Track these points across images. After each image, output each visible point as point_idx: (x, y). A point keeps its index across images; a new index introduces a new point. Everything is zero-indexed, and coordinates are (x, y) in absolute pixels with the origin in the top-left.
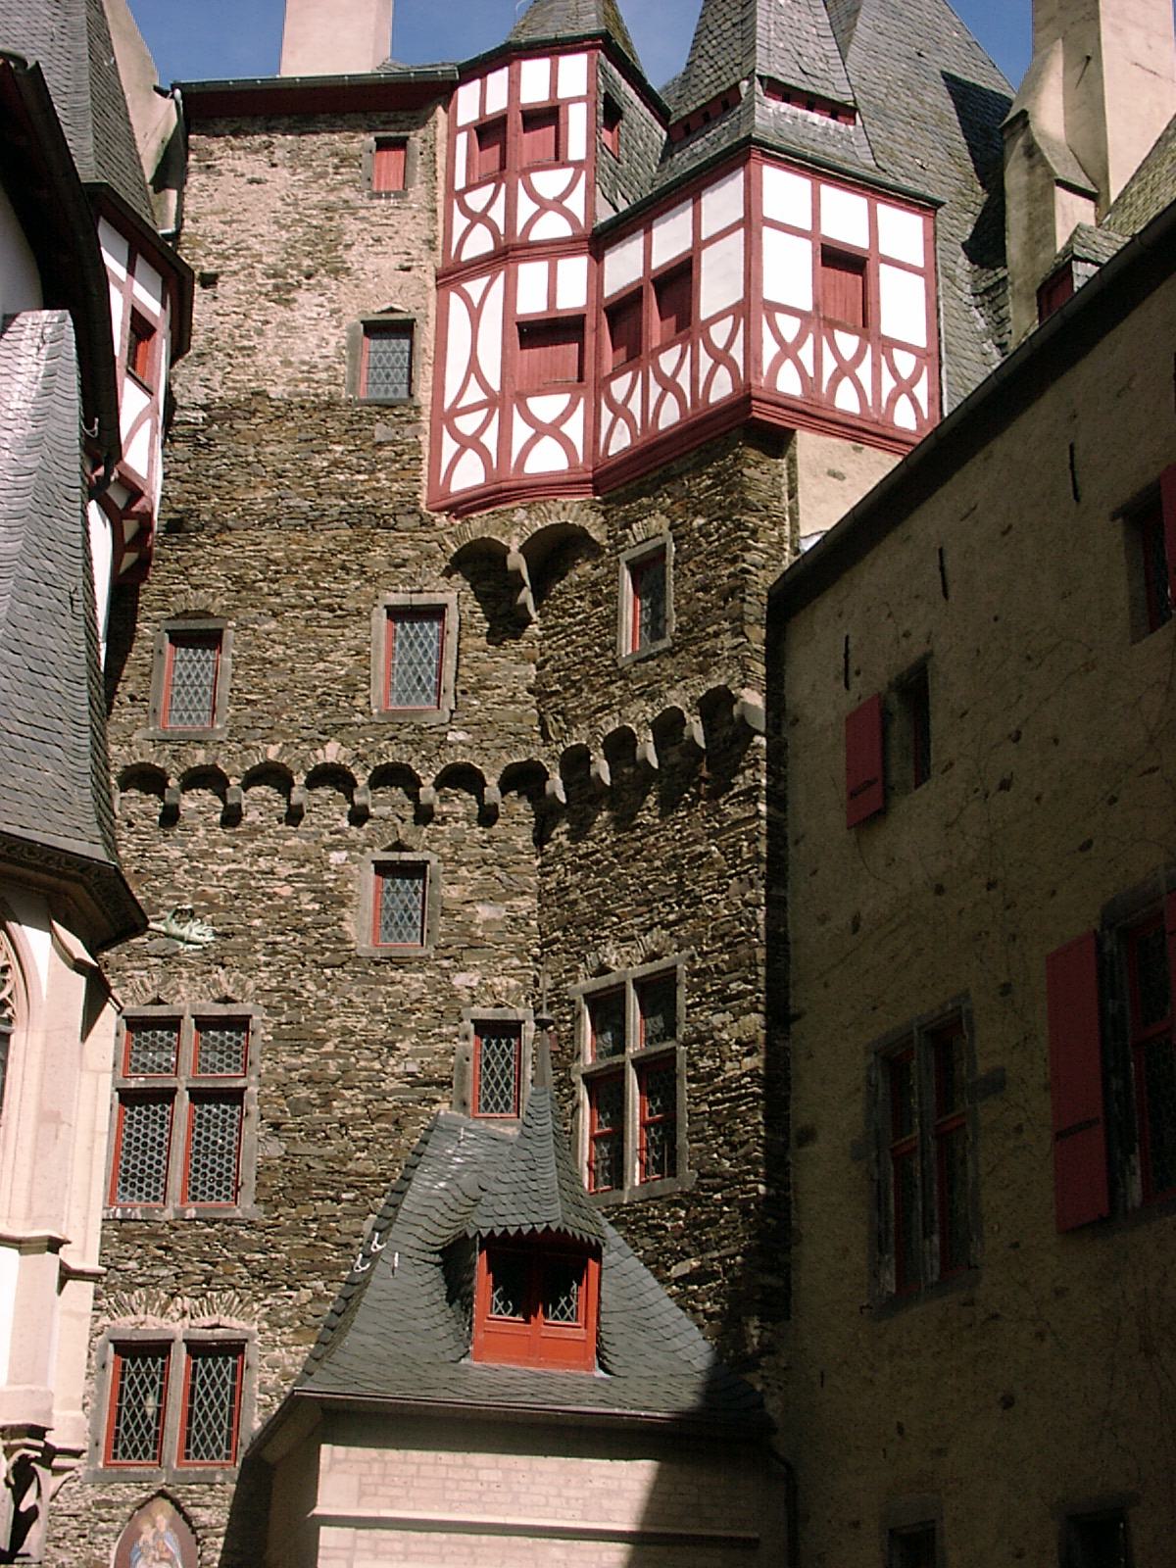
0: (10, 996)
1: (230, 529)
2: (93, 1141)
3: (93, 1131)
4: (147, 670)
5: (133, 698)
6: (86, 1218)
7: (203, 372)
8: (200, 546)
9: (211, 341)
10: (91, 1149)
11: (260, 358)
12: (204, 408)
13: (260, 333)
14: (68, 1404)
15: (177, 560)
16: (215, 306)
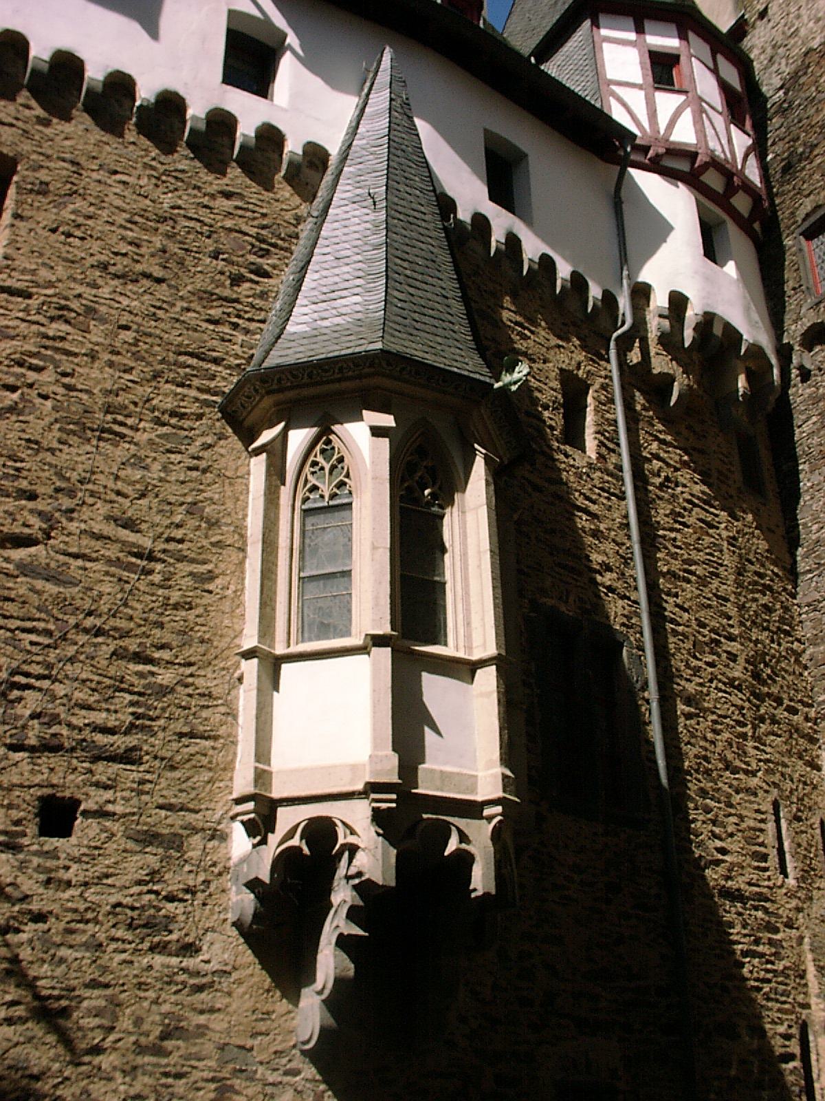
0: (345, 477)
1: (816, 146)
2: (480, 560)
3: (479, 552)
4: (796, 266)
5: (794, 289)
6: (483, 619)
7: (775, 68)
8: (803, 169)
9: (774, 47)
10: (479, 566)
11: (803, 32)
12: (781, 88)
13: (798, 17)
14: (488, 767)
15: (794, 189)
16: (771, 24)
